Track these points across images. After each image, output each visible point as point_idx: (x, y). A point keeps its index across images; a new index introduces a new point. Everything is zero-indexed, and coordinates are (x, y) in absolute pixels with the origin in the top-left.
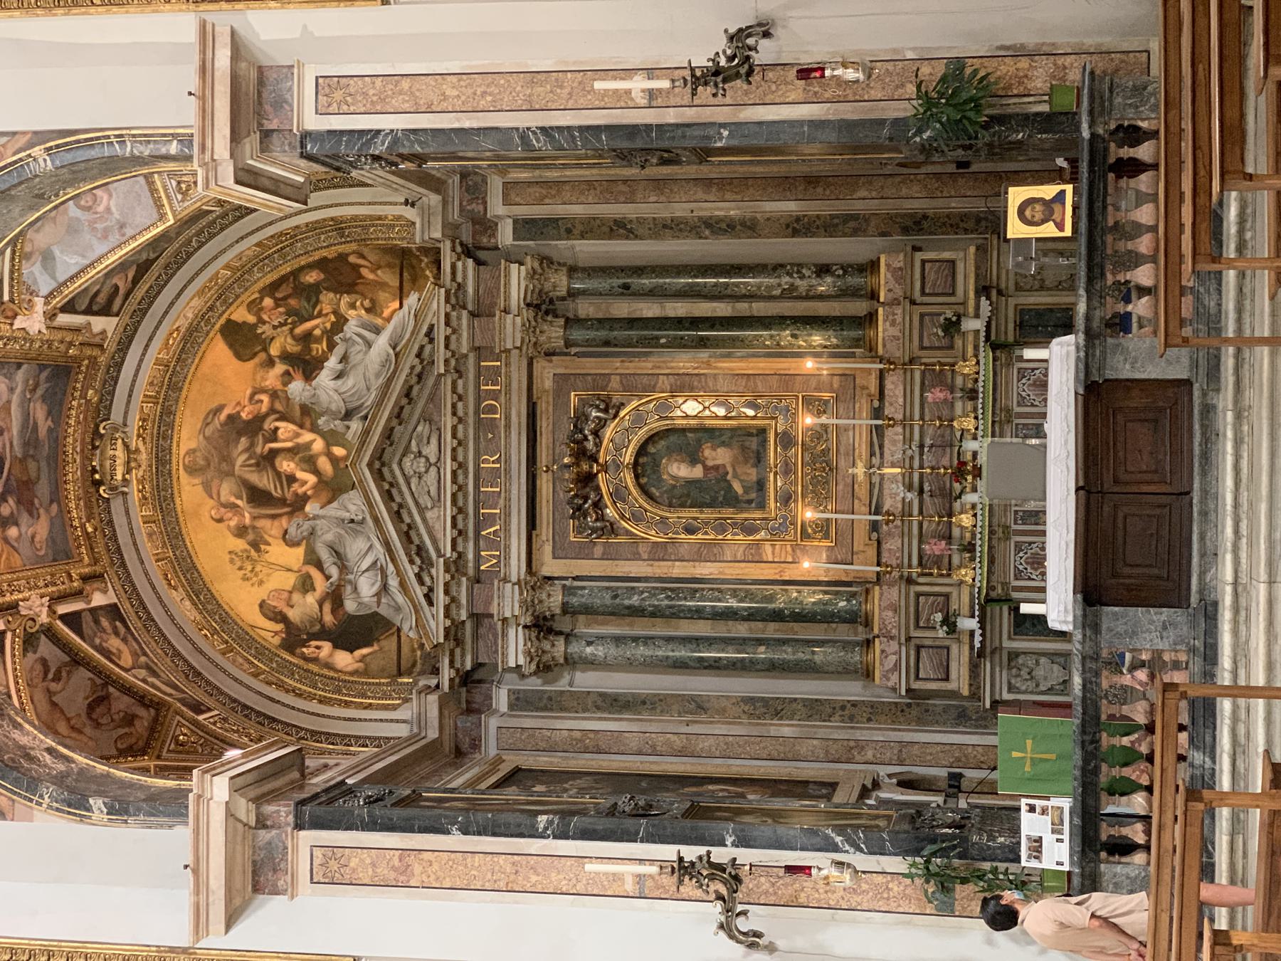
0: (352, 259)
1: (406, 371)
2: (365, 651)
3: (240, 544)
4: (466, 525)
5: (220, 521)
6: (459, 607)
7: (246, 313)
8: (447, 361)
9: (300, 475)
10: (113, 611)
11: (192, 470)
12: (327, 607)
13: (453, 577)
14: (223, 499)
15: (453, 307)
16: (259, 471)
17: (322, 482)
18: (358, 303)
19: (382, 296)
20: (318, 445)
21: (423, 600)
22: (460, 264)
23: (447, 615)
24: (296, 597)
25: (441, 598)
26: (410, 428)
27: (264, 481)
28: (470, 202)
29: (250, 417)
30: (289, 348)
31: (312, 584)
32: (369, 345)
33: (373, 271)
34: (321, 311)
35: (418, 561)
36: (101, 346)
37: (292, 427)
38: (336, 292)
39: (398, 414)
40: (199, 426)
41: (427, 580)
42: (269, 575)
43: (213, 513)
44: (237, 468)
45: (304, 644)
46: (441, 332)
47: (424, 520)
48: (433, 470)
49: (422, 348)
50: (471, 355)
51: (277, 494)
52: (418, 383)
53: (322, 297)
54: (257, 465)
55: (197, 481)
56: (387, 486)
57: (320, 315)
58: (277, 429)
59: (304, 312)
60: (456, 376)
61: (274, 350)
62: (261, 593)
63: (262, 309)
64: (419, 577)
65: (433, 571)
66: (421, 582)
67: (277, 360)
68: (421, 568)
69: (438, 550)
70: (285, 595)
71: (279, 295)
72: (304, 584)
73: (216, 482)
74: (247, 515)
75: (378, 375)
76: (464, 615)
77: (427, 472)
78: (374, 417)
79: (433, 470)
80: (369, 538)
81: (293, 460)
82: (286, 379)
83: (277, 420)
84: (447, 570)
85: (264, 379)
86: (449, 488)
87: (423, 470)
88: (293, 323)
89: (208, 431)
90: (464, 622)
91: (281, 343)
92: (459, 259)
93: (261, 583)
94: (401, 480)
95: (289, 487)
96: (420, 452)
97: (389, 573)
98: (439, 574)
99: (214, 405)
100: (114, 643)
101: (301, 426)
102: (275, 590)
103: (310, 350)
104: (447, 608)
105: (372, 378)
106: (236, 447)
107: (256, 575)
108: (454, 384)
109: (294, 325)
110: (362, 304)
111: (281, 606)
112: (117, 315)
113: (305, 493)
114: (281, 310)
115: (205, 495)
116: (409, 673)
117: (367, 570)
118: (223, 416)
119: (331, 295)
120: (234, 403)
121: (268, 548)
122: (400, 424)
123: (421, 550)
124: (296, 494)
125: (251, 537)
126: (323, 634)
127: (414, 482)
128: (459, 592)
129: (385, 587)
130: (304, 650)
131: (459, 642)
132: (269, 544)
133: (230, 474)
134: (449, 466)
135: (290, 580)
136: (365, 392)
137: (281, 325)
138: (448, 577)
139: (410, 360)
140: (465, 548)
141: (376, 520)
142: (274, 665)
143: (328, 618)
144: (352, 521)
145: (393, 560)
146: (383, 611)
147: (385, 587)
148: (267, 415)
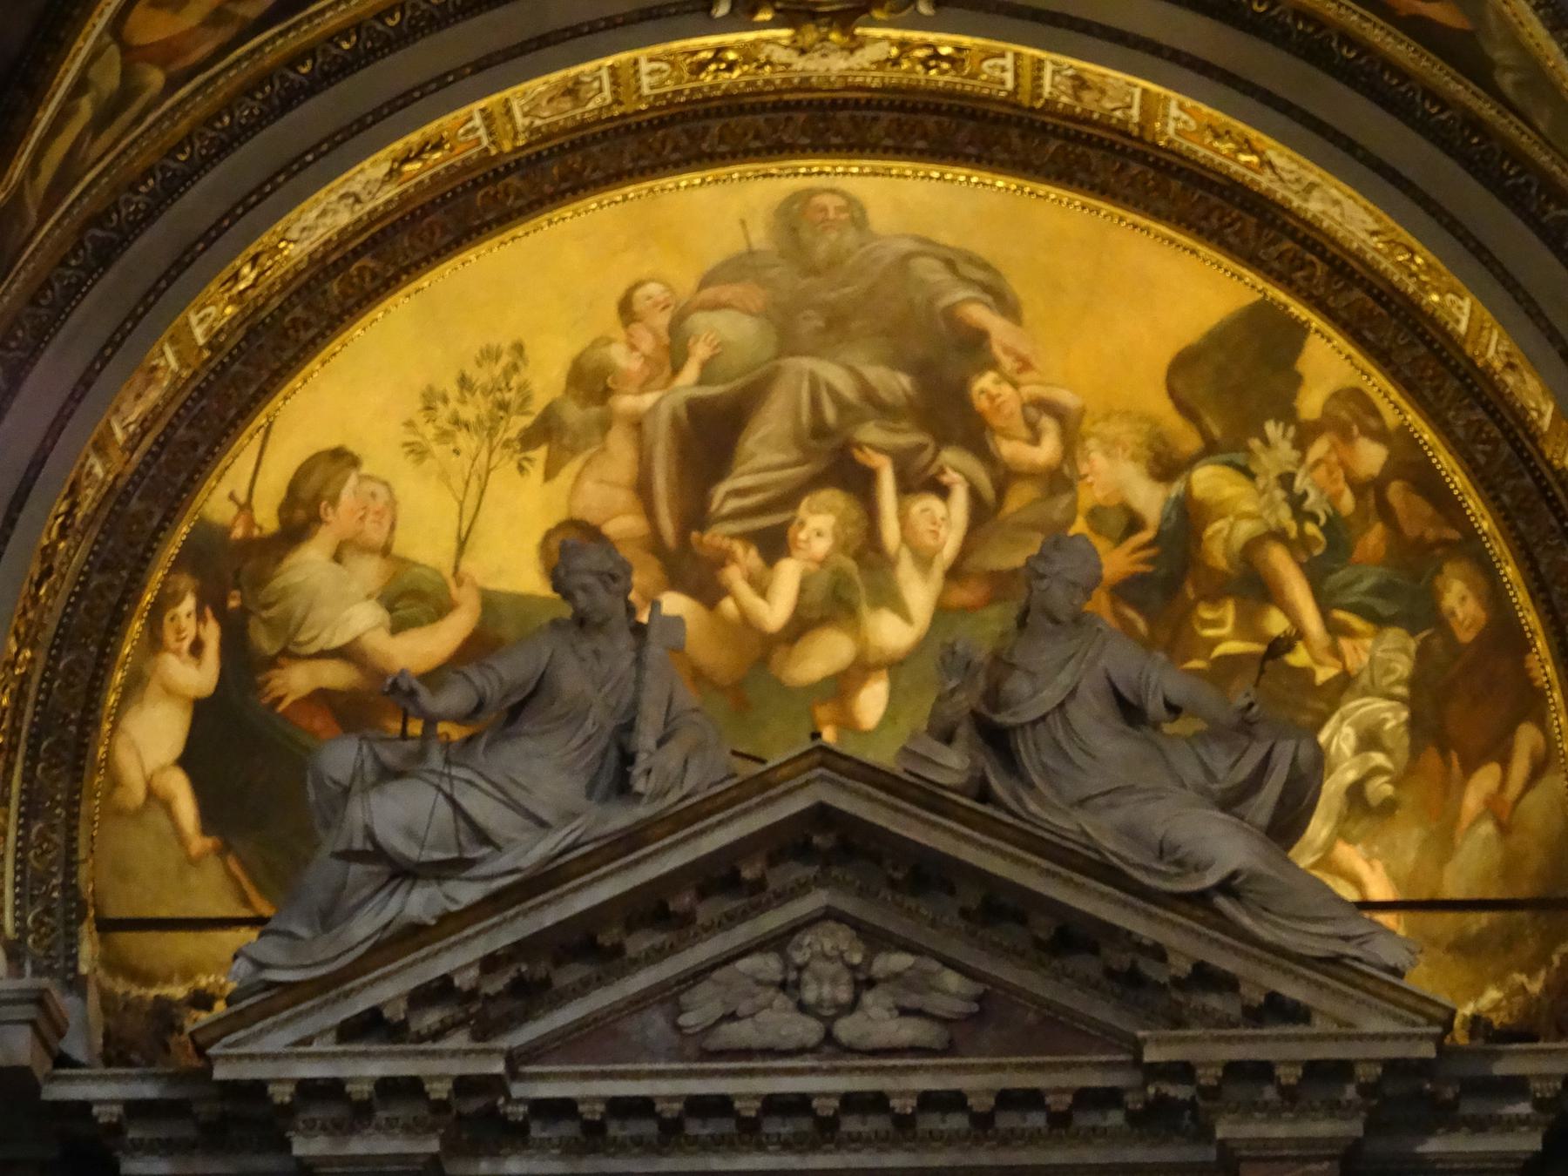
0: (1527, 738)
2: (186, 808)
5: (627, 310)
6: (340, 1129)
8: (1183, 1071)
9: (788, 574)
12: (335, 675)
13: (441, 1107)
14: (700, 320)
15: (1365, 1090)
16: (797, 440)
21: (361, 1004)
22: (1524, 1108)
23: (308, 1090)
24: (369, 571)
29: (982, 403)
30: (1217, 527)
32: (1232, 801)
33: (1492, 807)
34: (1350, 633)
37: (949, 548)
38: (1413, 682)
41: (431, 1018)
42: (444, 477)
43: (653, 289)
44: (807, 363)
45: (212, 601)
47: (639, 1003)
48: (807, 1030)
49: (1227, 983)
51: (722, 497)
52: (1110, 973)
54: (820, 430)
55: (760, 237)
56: (748, 873)
57: (1335, 630)
58: (943, 492)
59: (1341, 576)
60: (1134, 1101)
61: (1208, 480)
63: (1346, 437)
64: (440, 991)
66: (422, 997)
67: (1177, 488)
68: (472, 994)
69: (534, 1052)
70: (376, 535)
72: (415, 594)
73: (756, 297)
74: (649, 399)
75: (1130, 833)
76: (305, 1147)
77: (802, 1007)
78: (989, 826)
79: (807, 1030)
81: (841, 546)
82: (1116, 522)
83: (974, 494)
84: (464, 1085)
85: (1110, 447)
86: (747, 1088)
87: (810, 995)
89: (930, 270)
90: (286, 1146)
92: (1539, 1104)
93: (418, 452)
94: (772, 921)
95: (750, 537)
96: (871, 983)
99: (1018, 285)
102: (393, 503)
103: (1214, 599)
104: (333, 1089)
105: (1118, 816)
107: (444, 436)
108: (1107, 1098)
111: (340, 519)
113: (724, 591)
114: (1347, 502)
115: (714, 258)
116: (115, 964)
118: (980, 314)
119: (1403, 667)
120: (1024, 349)
121: (536, 472)
125: (573, 413)
127: (767, 965)
128: (389, 1127)
129: (403, 872)
130: (189, 604)
132: (550, 474)
133: (788, 344)
137: (1296, 503)
138: (440, 1090)
140: (542, 1147)
141: (630, 841)
142: (135, 505)
143: (297, 680)
144: (627, 758)
145: (495, 902)
146: (322, 872)
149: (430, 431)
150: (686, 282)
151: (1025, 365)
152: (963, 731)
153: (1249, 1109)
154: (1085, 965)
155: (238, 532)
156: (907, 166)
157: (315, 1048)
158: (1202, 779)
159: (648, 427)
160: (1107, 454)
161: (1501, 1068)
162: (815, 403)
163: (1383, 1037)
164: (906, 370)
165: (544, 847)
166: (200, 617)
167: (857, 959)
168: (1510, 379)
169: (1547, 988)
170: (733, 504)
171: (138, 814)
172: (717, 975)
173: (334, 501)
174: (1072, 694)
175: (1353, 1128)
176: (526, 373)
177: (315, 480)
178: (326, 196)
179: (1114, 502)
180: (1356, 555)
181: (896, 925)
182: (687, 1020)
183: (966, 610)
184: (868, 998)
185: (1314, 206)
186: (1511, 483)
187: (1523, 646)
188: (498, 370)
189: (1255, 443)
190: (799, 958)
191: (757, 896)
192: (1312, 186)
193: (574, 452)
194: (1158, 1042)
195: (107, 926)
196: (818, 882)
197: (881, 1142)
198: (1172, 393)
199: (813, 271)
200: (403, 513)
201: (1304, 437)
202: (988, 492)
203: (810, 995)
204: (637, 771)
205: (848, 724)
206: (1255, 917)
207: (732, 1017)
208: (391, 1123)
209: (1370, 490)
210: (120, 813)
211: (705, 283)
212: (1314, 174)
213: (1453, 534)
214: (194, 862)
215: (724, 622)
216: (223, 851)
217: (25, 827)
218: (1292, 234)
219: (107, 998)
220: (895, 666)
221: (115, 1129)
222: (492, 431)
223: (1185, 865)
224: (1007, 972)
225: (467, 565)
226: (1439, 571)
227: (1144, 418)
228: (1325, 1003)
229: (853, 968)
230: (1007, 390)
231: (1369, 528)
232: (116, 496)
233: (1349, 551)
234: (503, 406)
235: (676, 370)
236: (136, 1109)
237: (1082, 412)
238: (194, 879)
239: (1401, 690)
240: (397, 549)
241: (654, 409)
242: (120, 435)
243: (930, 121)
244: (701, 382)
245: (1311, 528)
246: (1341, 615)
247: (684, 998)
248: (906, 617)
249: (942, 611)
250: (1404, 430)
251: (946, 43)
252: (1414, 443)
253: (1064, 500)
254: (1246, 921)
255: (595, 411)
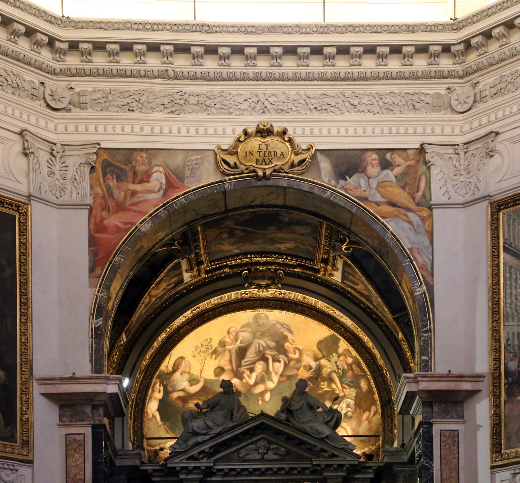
0: (373, 408)
1: (313, 443)
2: (158, 417)
3: (215, 344)
4: (230, 476)
5: (228, 332)
6: (187, 474)
7: (344, 348)
8: (319, 465)
9: (254, 375)
10: (181, 281)
11: (256, 318)
12: (181, 394)
13: (203, 470)
14: (240, 334)
16: (256, 353)
17: (251, 387)
18: (349, 409)
19: (354, 423)
20: (271, 385)
21: (191, 454)
22: (371, 471)
23: (182, 468)
24: (186, 376)
25: (192, 465)
26: (283, 444)
27: (251, 355)
28: (404, 477)
29: (286, 348)
31: (194, 385)
32: (327, 423)
33: (367, 419)
34: (346, 388)
35: (212, 450)
36: (325, 274)
37: (281, 370)
38: (356, 397)
39: (289, 438)
40: (281, 321)
41: (201, 456)
42: (198, 360)
43: (233, 329)
44: (258, 340)
45: (162, 383)
46: (334, 462)
49: (326, 451)
50: (322, 477)
51: (243, 362)
52: (308, 449)
53: (353, 389)
54: (260, 351)
55: (251, 320)
56: (251, 432)
57: (343, 388)
58: (280, 362)
59: (344, 379)
60: (311, 469)
61: (323, 362)
62: (188, 357)
63: (346, 356)
64: (203, 451)
65: (205, 460)
66: (200, 453)
67: (318, 363)
68: (208, 452)
70: (187, 370)
71: (354, 366)
72: (194, 380)
73: (250, 330)
74: (232, 347)
75: (311, 428)
76: (181, 477)
77: (259, 453)
80: (223, 424)
81: (263, 371)
82: (308, 368)
83: (285, 362)
85: (307, 355)
86: (251, 467)
87: (260, 451)
88: (338, 373)
89: (279, 326)
90: (178, 476)
91: (327, 366)
92: (374, 470)
93: (194, 356)
94: (254, 439)
95: (248, 369)
96: (270, 449)
97: (205, 437)
98: (204, 463)
99: (293, 329)
100: (163, 285)
101: (281, 375)
102: (190, 365)
103: (323, 381)
104: (186, 468)
105: (310, 425)
106: (270, 340)
107: (198, 353)
108: (307, 468)
109: (337, 373)
110: (349, 411)
111: (182, 368)
112: (342, 282)
113: (244, 378)
114: (346, 367)
116: (148, 445)
117: (207, 425)
118: (287, 333)
119: (354, 394)
120: (293, 339)
121: (213, 359)
122: (285, 439)
123: (216, 452)
124: (243, 373)
125: (219, 349)
126: (167, 393)
128: (195, 474)
130: (158, 384)
131: (167, 475)
132: (215, 359)
133: (255, 337)
134: (262, 466)
135: (195, 371)
136: (302, 421)
137: (337, 366)
138: (203, 468)
139: (320, 446)
140: (218, 476)
142: (150, 369)
143: (175, 395)
147: (195, 434)
148: (287, 356)
149: (196, 353)
150: (238, 328)
151: (294, 342)
152: (285, 411)
153: (329, 471)
154: (303, 447)
155: (166, 372)
156: (276, 311)
157: (183, 461)
158: (323, 419)
159: (232, 351)
160: (307, 357)
161: (368, 465)
162: (259, 347)
163: (350, 460)
164: (274, 342)
165: (219, 429)
166: (160, 386)
167: (268, 446)
168: (373, 350)
169: (375, 449)
170: (245, 364)
171: (151, 419)
172: (246, 448)
173: (181, 365)
174: (302, 406)
175: (344, 474)
176: (212, 343)
177: (178, 362)
178: (181, 317)
179: (307, 364)
180: (347, 376)
181: (273, 440)
182: (241, 455)
183: (282, 381)
184: (269, 452)
185: (342, 320)
186: (372, 367)
187: (374, 393)
188: (207, 343)
189: (331, 356)
190: (259, 446)
191: (252, 436)
192: (342, 317)
193: (219, 355)
194: (315, 461)
195: (147, 439)
196: (262, 433)
197: (272, 475)
198: (318, 347)
199: (259, 326)
200: (192, 367)
201: (339, 356)
202: (287, 362)
203: (260, 451)
204: (234, 417)
205: (263, 400)
206: (331, 441)
207: (248, 454)
208: (195, 473)
209: (350, 365)
210: (148, 419)
211: (241, 328)
212: (342, 315)
213: (363, 374)
214: (160, 426)
215: (244, 383)
216: (164, 424)
217: (134, 423)
218: (338, 323)
219: (147, 450)
220: (271, 391)
221: (151, 474)
222: (206, 352)
223: (320, 433)
224: (292, 448)
225: (202, 375)
226: (360, 379)
227: (313, 351)
228: (341, 455)
229: (267, 447)
230: (290, 346)
231: (349, 372)
232: (147, 367)
233: (346, 375)
234: (208, 348)
235: (236, 342)
236: (155, 471)
237: (303, 350)
238: (160, 429)
239: (353, 398)
240: (191, 372)
241: (233, 348)
242: (148, 357)
243: (279, 303)
244: (241, 343)
245: (340, 371)
246: (344, 385)
247: (240, 451)
248: (273, 382)
249: (279, 382)
250: (355, 356)
251: (283, 291)
252: (357, 359)
253: (299, 364)
254: (329, 442)
255: (223, 349)
